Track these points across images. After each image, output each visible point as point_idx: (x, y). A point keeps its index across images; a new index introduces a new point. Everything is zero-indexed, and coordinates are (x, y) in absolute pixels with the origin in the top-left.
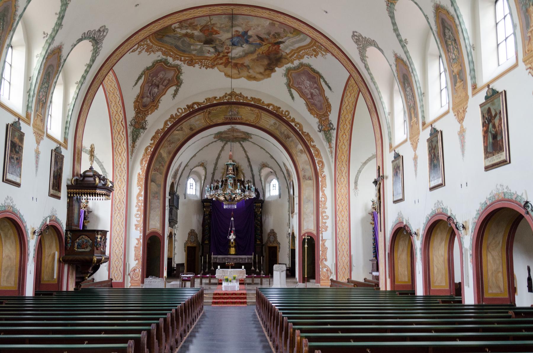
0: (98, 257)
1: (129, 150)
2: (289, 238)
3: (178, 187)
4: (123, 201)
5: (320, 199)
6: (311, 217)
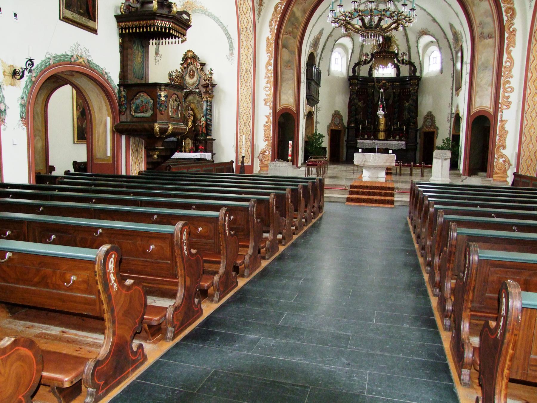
0: (163, 125)
1: (256, 9)
2: (451, 122)
3: (321, 61)
4: (250, 72)
5: (504, 64)
6: (487, 90)
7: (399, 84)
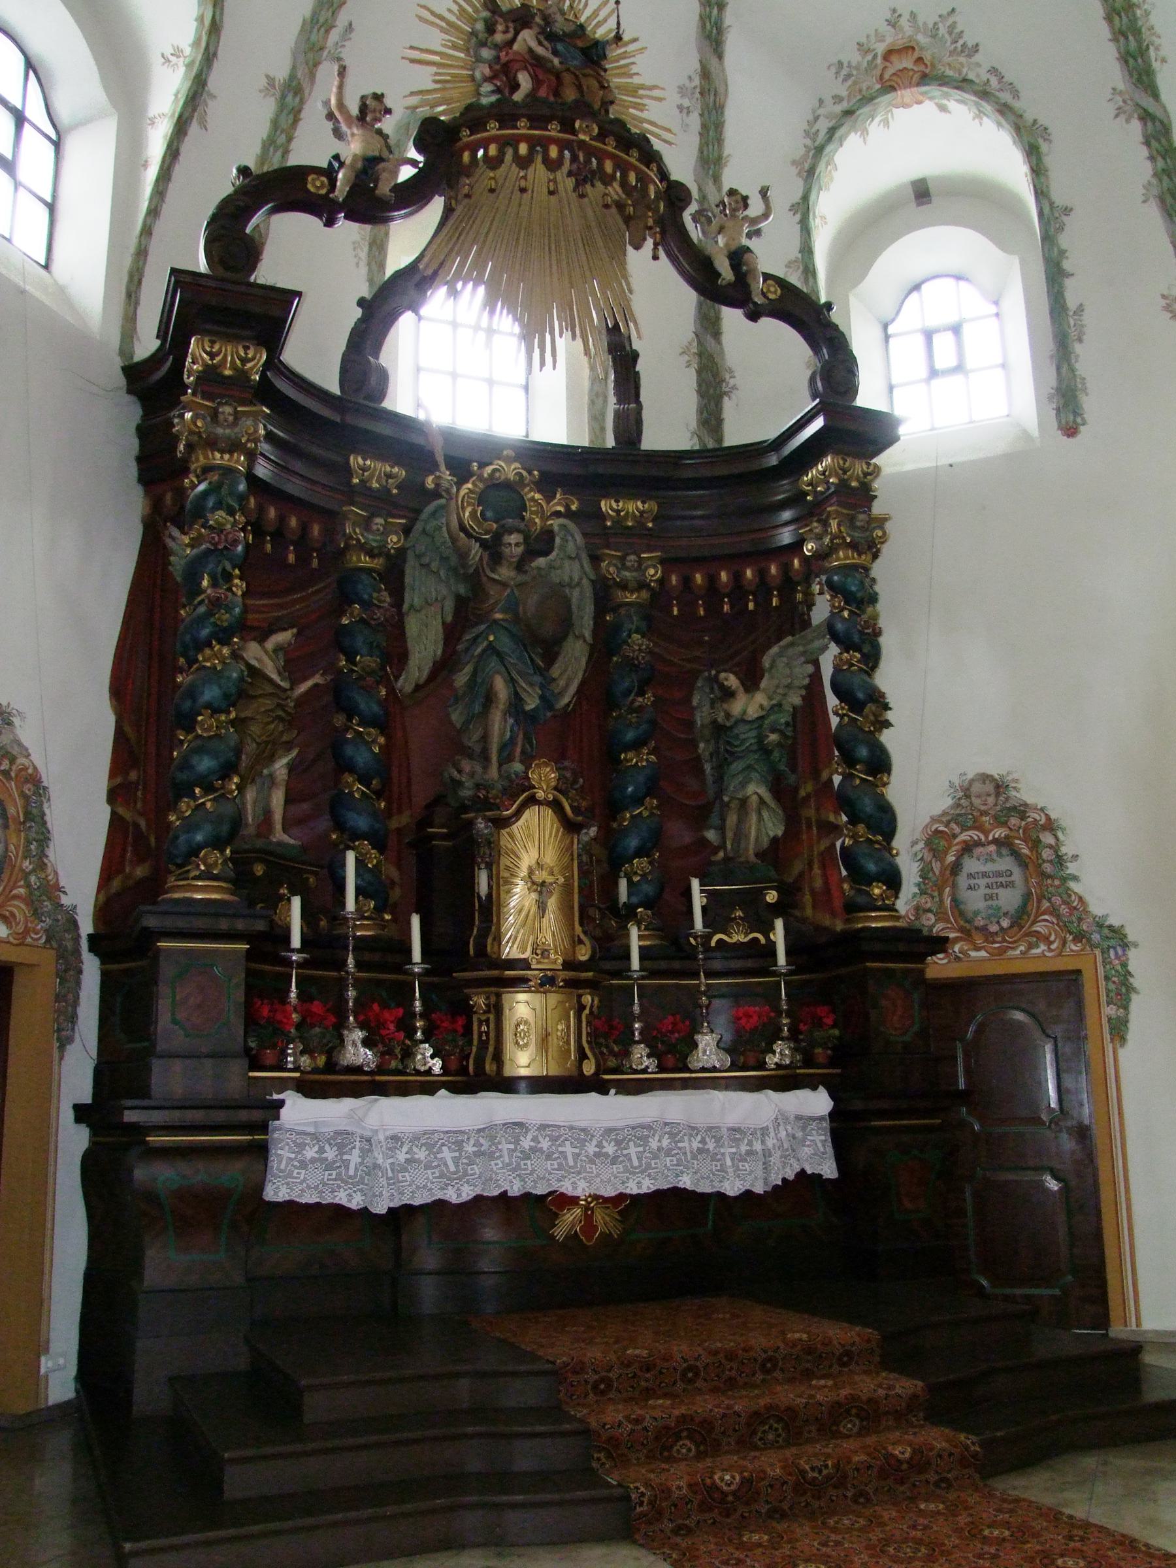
7: (651, 506)
